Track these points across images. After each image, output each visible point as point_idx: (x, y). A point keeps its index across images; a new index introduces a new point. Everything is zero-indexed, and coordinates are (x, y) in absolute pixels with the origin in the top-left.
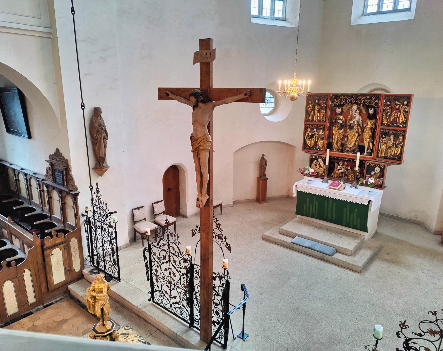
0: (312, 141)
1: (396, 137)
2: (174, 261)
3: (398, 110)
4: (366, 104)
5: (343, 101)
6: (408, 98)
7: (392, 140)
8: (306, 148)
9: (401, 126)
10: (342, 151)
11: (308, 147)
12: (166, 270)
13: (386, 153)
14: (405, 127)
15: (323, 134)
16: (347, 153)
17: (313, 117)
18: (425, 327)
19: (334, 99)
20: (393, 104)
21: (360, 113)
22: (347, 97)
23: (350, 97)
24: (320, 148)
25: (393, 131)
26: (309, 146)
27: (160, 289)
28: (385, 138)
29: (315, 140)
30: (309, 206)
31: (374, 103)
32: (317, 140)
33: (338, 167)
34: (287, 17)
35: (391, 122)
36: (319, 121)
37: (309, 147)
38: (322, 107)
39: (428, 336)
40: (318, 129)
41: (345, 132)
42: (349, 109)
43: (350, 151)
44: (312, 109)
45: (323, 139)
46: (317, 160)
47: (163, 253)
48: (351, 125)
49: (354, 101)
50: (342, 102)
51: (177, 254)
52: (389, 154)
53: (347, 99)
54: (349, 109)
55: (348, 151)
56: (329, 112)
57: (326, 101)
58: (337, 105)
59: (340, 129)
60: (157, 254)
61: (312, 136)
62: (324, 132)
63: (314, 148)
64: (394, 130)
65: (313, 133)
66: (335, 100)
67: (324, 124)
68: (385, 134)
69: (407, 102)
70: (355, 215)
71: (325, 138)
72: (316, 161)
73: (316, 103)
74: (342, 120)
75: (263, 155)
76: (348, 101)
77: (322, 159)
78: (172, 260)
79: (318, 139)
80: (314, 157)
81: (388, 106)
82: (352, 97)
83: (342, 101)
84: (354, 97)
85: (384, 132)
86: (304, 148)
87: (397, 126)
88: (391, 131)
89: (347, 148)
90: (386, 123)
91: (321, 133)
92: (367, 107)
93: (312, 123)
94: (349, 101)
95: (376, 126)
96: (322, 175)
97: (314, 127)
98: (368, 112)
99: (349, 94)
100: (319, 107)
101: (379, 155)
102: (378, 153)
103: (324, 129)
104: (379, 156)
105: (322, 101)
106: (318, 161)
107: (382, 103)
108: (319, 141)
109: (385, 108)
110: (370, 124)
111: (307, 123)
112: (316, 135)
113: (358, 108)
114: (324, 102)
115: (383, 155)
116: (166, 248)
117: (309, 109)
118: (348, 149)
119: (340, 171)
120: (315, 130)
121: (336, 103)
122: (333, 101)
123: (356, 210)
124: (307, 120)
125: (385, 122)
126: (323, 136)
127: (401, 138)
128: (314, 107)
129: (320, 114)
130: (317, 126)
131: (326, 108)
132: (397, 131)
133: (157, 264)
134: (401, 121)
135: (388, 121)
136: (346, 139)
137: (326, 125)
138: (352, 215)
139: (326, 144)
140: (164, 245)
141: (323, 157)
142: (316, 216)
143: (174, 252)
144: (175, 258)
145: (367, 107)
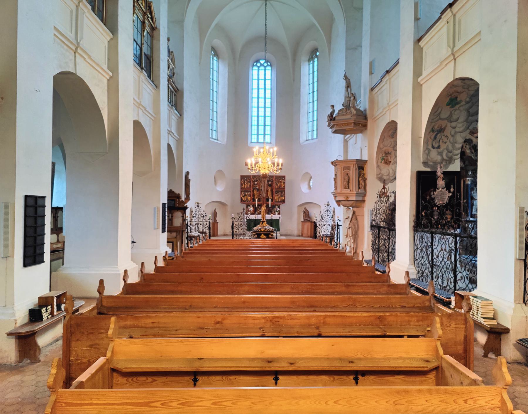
1: (282, 193)
3: (281, 182)
6: (284, 177)
12: (242, 229)
13: (278, 200)
17: (244, 186)
18: (325, 211)
24: (249, 201)
36: (248, 188)
39: (325, 212)
40: (248, 192)
45: (250, 196)
47: (241, 223)
52: (279, 200)
56: (252, 183)
60: (237, 224)
61: (245, 196)
68: (277, 192)
75: (215, 209)
91: (249, 194)
95: (273, 189)
98: (269, 183)
103: (250, 192)
116: (243, 220)
124: (241, 188)
125: (277, 187)
127: (283, 193)
128: (244, 181)
131: (250, 182)
133: (237, 229)
140: (241, 219)
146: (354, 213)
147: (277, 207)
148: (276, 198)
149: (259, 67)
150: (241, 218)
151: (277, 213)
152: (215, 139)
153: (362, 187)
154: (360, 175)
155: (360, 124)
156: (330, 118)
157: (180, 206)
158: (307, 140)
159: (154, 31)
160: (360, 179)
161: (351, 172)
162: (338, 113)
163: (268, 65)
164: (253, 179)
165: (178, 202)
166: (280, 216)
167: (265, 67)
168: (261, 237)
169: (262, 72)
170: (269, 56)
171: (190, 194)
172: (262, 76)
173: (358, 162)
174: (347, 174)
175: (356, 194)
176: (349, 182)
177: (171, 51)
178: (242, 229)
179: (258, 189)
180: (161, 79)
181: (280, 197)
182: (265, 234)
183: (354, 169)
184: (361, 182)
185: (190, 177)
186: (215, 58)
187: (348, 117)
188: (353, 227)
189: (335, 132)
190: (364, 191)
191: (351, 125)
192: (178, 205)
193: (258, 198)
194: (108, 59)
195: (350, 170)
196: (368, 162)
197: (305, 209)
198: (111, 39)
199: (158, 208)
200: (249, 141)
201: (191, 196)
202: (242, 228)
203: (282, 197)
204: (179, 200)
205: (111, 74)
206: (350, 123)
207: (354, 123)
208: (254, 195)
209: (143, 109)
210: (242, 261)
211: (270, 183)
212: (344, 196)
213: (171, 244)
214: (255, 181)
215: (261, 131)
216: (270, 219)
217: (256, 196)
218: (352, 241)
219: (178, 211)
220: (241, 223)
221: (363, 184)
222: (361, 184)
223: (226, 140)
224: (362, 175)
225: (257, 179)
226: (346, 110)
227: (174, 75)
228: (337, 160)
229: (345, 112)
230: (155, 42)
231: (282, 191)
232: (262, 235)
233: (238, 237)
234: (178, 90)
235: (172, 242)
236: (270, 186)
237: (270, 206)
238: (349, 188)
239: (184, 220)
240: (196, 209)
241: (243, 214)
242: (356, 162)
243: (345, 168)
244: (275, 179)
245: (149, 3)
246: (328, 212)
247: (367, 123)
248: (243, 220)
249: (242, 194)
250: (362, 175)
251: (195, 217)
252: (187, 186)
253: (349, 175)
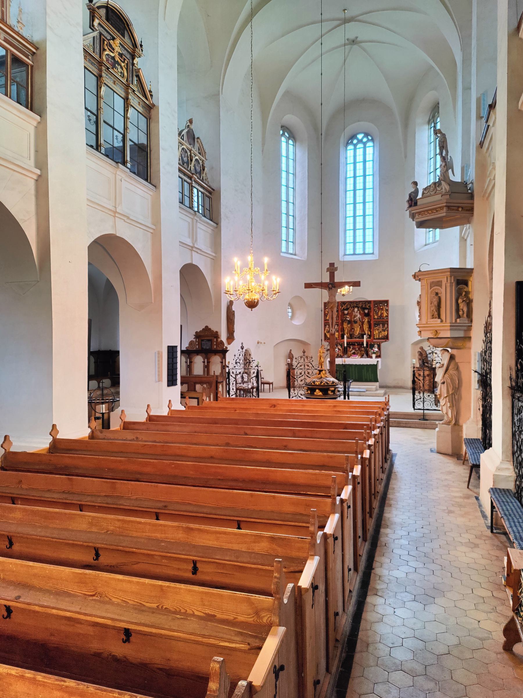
1: (384, 326)
2: (308, 373)
6: (387, 302)
10: (351, 338)
12: (301, 381)
13: (379, 336)
20: (379, 306)
21: (360, 313)
27: (296, 395)
34: (297, 253)
35: (379, 317)
41: (352, 325)
42: (352, 311)
45: (338, 331)
47: (300, 371)
51: (311, 368)
52: (381, 336)
54: (352, 311)
55: (355, 337)
59: (348, 324)
68: (377, 324)
70: (370, 373)
75: (291, 350)
78: (306, 372)
81: (376, 307)
86: (325, 339)
87: (383, 319)
92: (364, 309)
95: (371, 320)
98: (365, 312)
101: (375, 337)
107: (372, 305)
110: (366, 320)
113: (358, 310)
115: (377, 337)
116: (303, 367)
119: (352, 352)
123: (370, 369)
125: (376, 317)
127: (386, 325)
134: (385, 316)
140: (301, 366)
143: (308, 368)
144: (309, 371)
145: (364, 309)
146: (452, 358)
147: (376, 346)
148: (376, 332)
149: (355, 145)
150: (300, 364)
151: (374, 356)
152: (291, 254)
153: (463, 314)
154: (459, 294)
155: (459, 207)
156: (409, 203)
157: (218, 349)
158: (426, 245)
159: (152, 110)
160: (460, 301)
161: (443, 290)
162: (423, 193)
163: (368, 140)
164: (342, 306)
165: (215, 343)
166: (379, 359)
167: (365, 144)
168: (315, 393)
169: (360, 152)
170: (365, 125)
171: (234, 331)
172: (360, 158)
173: (453, 272)
174: (437, 294)
175: (451, 326)
176: (439, 306)
177: (196, 137)
178: (301, 381)
180: (161, 174)
181: (381, 332)
182: (321, 390)
183: (448, 285)
184: (463, 306)
185: (234, 308)
186: (291, 142)
187: (438, 197)
188: (449, 381)
189: (420, 225)
190: (467, 322)
191: (442, 211)
192: (215, 347)
193: (350, 334)
194: (36, 151)
195: (441, 286)
196: (475, 274)
197: (422, 348)
198: (39, 123)
199: (160, 354)
200: (341, 253)
201: (235, 334)
202: (302, 378)
203: (384, 331)
204: (217, 340)
205: (38, 172)
206: (440, 208)
207: (448, 207)
208: (343, 330)
209: (125, 219)
210: (155, 445)
211: (366, 311)
212: (430, 330)
213: (196, 400)
214: (344, 310)
215: (360, 238)
216: (343, 364)
217: (346, 331)
218: (449, 404)
219: (215, 355)
220: (300, 371)
221: (465, 309)
222: (462, 309)
223: (306, 254)
224: (464, 293)
225: (347, 306)
226: (435, 187)
227: (204, 170)
228: (420, 271)
229: (434, 190)
230: (152, 125)
231: (384, 322)
232: (317, 390)
233: (296, 392)
234: (214, 190)
235: (198, 398)
236: (366, 316)
237: (365, 345)
238: (439, 317)
239: (224, 367)
240: (240, 351)
241: (303, 359)
242: (450, 272)
243: (433, 284)
244: (374, 305)
245: (137, 71)
246: (434, 354)
247: (473, 204)
248: (303, 367)
249: (326, 329)
250: (464, 293)
251: (239, 363)
252: (230, 321)
253: (439, 295)
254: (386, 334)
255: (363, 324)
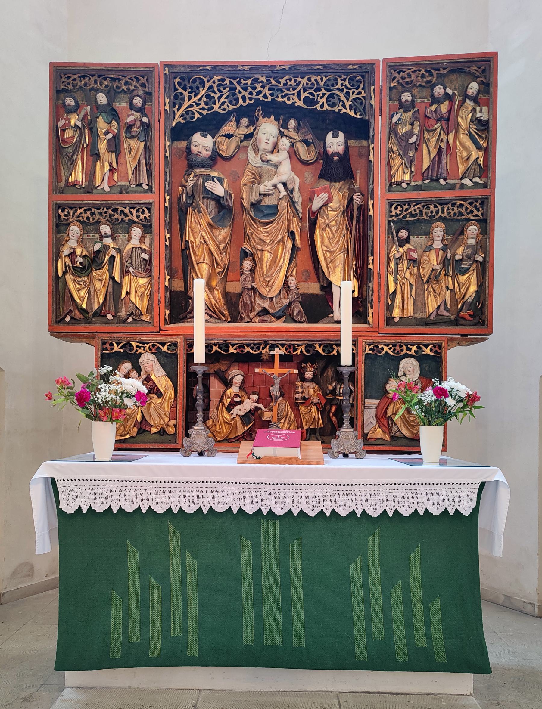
0: (98, 285)
4: (318, 107)
5: (219, 98)
7: (438, 245)
8: (68, 319)
9: (467, 182)
10: (235, 318)
11: (77, 314)
14: (485, 186)
15: (143, 247)
16: (264, 321)
17: (90, 175)
19: (181, 90)
20: (422, 101)
22: (234, 82)
23: (249, 82)
24: (135, 314)
25: (440, 207)
26: (84, 306)
28: (407, 241)
29: (112, 278)
30: (144, 598)
31: (348, 104)
32: (117, 279)
33: (224, 393)
35: (423, 175)
36: (124, 190)
37: (84, 311)
38: (130, 127)
43: (272, 311)
44: (81, 135)
46: (134, 359)
48: (263, 204)
49: (265, 96)
50: (218, 104)
52: (432, 305)
53: (239, 88)
55: (265, 312)
57: (144, 103)
58: (197, 116)
62: (147, 240)
63: (109, 317)
64: (443, 203)
65: (98, 246)
66: (186, 94)
67: (144, 198)
69: (481, 83)
71: (155, 263)
72: (127, 366)
73: (98, 108)
74: (221, 181)
76: (240, 96)
77: (158, 353)
79: (124, 272)
80: (116, 348)
81: (404, 107)
82: (256, 80)
83: (216, 97)
84: (264, 79)
85: (405, 217)
88: (432, 207)
89: (258, 301)
90: (407, 177)
91: (135, 242)
93: (87, 199)
94: (247, 96)
96: (162, 432)
97: (97, 216)
99: (244, 64)
100: (114, 123)
101: (396, 313)
102: (390, 308)
103: (147, 227)
104: (397, 320)
105: (124, 104)
106: (137, 368)
108: (127, 279)
109: (395, 119)
111: (61, 199)
112: (114, 253)
114: (138, 101)
117: (68, 134)
118: (266, 305)
119: (239, 411)
120: (105, 229)
121: (191, 106)
122: (178, 100)
126: (146, 257)
127: (473, 229)
129: (121, 160)
130: (115, 210)
132: (454, 205)
134: (462, 168)
135: (412, 172)
136: (247, 264)
137: (155, 206)
138: (396, 593)
139: (163, 290)
141: (163, 344)
142: (193, 650)
179: (218, 199)
181: (434, 277)
193: (226, 295)
249: (66, 251)
254: (473, 288)
255: (313, 225)
